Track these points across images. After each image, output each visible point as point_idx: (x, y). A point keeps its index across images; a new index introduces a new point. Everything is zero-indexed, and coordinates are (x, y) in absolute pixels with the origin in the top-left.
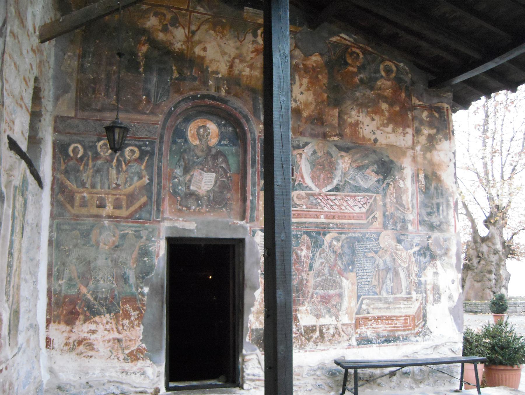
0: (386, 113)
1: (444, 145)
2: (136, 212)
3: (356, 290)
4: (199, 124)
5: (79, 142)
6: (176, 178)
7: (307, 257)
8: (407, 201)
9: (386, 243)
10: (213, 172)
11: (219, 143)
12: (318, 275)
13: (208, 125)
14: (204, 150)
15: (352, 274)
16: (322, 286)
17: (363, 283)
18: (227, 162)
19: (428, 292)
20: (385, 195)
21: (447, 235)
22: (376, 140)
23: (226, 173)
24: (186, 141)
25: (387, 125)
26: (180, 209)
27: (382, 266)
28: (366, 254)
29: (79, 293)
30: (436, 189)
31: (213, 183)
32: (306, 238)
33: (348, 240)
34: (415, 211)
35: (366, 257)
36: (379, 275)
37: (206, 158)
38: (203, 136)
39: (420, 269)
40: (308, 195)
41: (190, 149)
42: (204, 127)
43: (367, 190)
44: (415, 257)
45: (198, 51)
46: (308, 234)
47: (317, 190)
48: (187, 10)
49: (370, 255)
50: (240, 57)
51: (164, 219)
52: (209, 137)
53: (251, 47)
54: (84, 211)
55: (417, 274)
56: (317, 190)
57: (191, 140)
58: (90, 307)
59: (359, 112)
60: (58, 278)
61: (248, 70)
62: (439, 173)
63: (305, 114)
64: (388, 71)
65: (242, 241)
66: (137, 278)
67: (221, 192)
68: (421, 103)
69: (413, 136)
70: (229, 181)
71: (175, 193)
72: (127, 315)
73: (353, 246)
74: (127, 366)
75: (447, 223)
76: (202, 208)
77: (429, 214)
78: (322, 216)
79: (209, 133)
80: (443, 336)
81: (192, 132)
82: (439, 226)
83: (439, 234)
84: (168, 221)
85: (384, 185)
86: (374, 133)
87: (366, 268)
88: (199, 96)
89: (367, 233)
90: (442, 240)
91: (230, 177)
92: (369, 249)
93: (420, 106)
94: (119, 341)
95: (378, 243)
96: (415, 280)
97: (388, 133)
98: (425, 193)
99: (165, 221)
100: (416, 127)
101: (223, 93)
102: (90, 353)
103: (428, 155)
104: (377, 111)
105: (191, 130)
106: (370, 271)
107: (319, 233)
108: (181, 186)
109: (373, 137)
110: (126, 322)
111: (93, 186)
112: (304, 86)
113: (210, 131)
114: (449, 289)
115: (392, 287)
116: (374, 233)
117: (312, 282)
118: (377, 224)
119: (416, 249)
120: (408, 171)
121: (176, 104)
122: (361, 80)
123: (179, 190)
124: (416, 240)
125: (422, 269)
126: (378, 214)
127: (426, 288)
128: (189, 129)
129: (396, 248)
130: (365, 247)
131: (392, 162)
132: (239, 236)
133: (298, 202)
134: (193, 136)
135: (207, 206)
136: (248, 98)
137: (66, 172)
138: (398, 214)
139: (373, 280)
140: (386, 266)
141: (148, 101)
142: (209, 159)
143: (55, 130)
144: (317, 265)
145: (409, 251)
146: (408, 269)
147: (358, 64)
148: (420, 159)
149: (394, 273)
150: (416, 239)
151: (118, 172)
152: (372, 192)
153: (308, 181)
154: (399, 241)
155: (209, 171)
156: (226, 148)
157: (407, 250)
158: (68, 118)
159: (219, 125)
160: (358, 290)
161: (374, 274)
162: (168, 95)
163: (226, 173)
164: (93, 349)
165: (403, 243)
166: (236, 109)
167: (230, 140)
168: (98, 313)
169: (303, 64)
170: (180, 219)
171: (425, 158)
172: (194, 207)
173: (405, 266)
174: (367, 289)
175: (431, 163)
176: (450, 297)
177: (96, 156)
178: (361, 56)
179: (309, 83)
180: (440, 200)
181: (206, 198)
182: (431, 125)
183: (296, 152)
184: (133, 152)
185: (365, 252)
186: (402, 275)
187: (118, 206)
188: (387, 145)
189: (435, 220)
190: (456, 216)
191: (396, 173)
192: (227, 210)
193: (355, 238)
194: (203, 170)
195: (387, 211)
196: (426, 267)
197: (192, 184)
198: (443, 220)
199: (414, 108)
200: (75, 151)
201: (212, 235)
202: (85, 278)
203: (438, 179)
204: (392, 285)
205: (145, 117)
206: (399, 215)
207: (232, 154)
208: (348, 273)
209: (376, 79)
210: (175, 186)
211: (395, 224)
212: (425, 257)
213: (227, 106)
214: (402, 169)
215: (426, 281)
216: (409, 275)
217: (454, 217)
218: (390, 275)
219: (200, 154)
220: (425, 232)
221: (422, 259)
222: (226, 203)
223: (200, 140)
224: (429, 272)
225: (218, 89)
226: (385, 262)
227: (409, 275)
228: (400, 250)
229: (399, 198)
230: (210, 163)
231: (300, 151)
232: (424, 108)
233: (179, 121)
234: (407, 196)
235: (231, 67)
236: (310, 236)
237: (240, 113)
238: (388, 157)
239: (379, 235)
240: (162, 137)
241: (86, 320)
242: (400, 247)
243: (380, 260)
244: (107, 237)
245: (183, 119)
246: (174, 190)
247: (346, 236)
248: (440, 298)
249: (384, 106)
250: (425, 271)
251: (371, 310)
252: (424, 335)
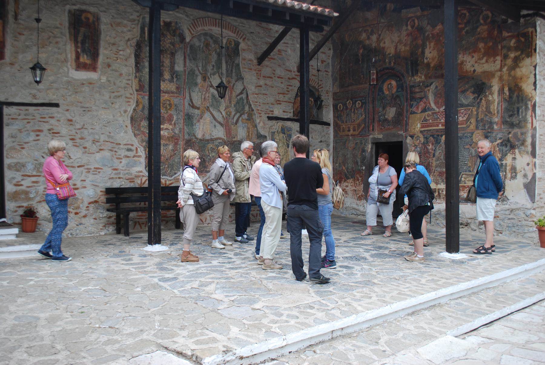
0: (482, 50)
1: (528, 61)
2: (360, 132)
5: (341, 103)
7: (432, 149)
8: (494, 109)
11: (397, 91)
12: (438, 159)
16: (440, 166)
18: (400, 100)
19: (508, 171)
20: (478, 108)
21: (524, 130)
22: (474, 71)
23: (400, 106)
24: (383, 93)
25: (482, 58)
27: (474, 154)
29: (342, 169)
30: (518, 97)
32: (431, 138)
34: (500, 115)
40: (433, 113)
43: (468, 105)
45: (382, 45)
46: (433, 136)
47: (437, 110)
48: (377, 23)
49: (467, 147)
50: (400, 41)
51: (371, 134)
53: (405, 33)
54: (343, 134)
56: (437, 110)
58: (346, 175)
59: (464, 55)
60: (336, 163)
61: (403, 47)
62: (520, 85)
63: (432, 65)
64: (486, 18)
65: (402, 142)
66: (361, 162)
68: (510, 34)
69: (501, 61)
71: (379, 121)
72: (358, 180)
74: (358, 202)
75: (525, 121)
77: (511, 116)
78: (440, 125)
80: (518, 203)
82: (518, 124)
83: (518, 130)
85: (478, 100)
86: (473, 66)
90: (519, 134)
93: (508, 37)
94: (355, 191)
95: (472, 139)
97: (483, 64)
98: (508, 102)
100: (504, 54)
101: (392, 64)
102: (347, 195)
103: (513, 73)
104: (476, 50)
107: (438, 135)
109: (472, 69)
110: (358, 182)
111: (346, 122)
112: (432, 48)
114: (524, 169)
117: (434, 164)
118: (472, 127)
119: (499, 141)
120: (496, 88)
122: (467, 32)
124: (499, 136)
125: (504, 156)
126: (473, 121)
127: (506, 169)
131: (484, 84)
132: (400, 140)
133: (428, 119)
137: (338, 117)
138: (487, 119)
141: (364, 77)
143: (333, 99)
144: (437, 154)
147: (465, 21)
148: (505, 77)
151: (354, 114)
152: (470, 106)
153: (433, 105)
155: (393, 107)
158: (338, 93)
159: (396, 81)
163: (400, 106)
164: (347, 194)
168: (348, 178)
169: (432, 34)
171: (510, 75)
175: (515, 78)
176: (525, 176)
177: (347, 109)
178: (467, 14)
179: (434, 44)
180: (521, 104)
182: (516, 49)
183: (426, 90)
184: (359, 103)
187: (354, 130)
188: (482, 72)
189: (515, 120)
190: (533, 115)
191: (487, 90)
195: (478, 117)
196: (507, 154)
198: (522, 120)
199: (504, 39)
200: (340, 108)
201: (389, 141)
202: (344, 162)
203: (520, 89)
205: (362, 86)
206: (487, 119)
209: (477, 27)
211: (484, 125)
212: (506, 147)
214: (491, 87)
217: (532, 116)
219: (389, 98)
221: (504, 148)
224: (509, 157)
225: (390, 63)
229: (488, 108)
231: (429, 88)
232: (512, 37)
234: (494, 106)
235: (396, 49)
236: (434, 138)
238: (481, 80)
239: (472, 134)
240: (369, 94)
241: (345, 181)
244: (351, 145)
248: (516, 176)
249: (481, 45)
251: (466, 181)
252: (503, 201)
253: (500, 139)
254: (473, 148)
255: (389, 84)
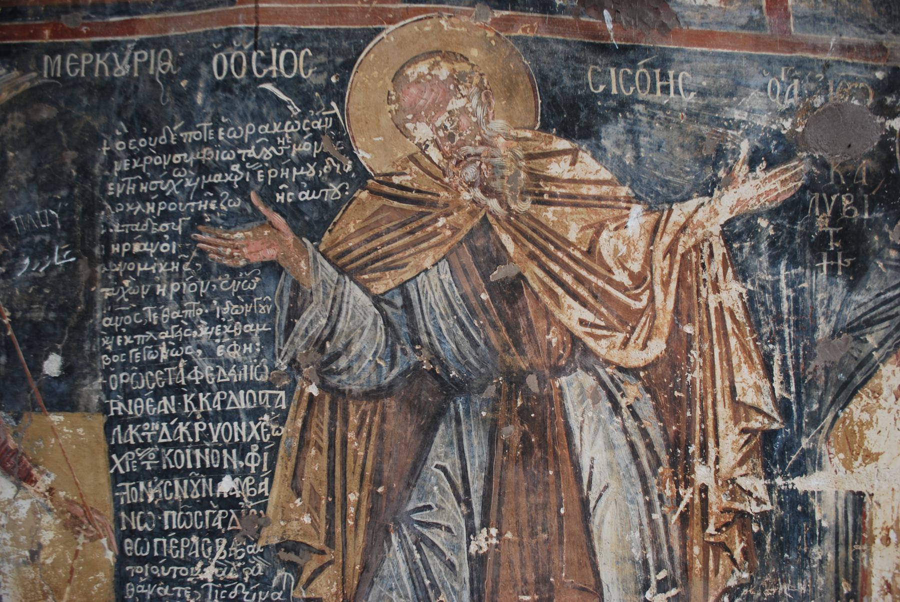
3: (104, 578)
9: (423, 132)
15: (69, 434)
17: (172, 518)
28: (204, 237)
33: (46, 113)
35: (206, 273)
36: (336, 449)
39: (804, 386)
44: (742, 274)
49: (248, 245)
55: (769, 436)
73: (84, 170)
87: (205, 371)
89: (228, 38)
92: (243, 190)
95: (339, 133)
96: (737, 492)
106: (241, 401)
115: (478, 562)
116: (295, 40)
119: (753, 190)
124: (760, 109)
129: (535, 177)
130: (202, 168)
139: (277, 493)
140: (407, 358)
145: (679, 213)
146: (667, 385)
149: (511, 432)
150: (755, 99)
154: (571, 115)
157: (659, 197)
160: (121, 579)
161: (289, 432)
165: (612, 134)
173: (636, 357)
174: (210, 573)
185: (198, 218)
186: (599, 445)
193: (105, 88)
196: (867, 368)
204: (482, 542)
208: (34, 422)
212: (856, 275)
215: (858, 501)
216: (677, 445)
218: (460, 451)
220: (851, 35)
221: (825, 291)
226: (400, 314)
227: (677, 445)
228: (574, 201)
242: (578, 167)
243: (354, 294)
247: (26, 82)
250: (856, 409)
253: (771, 154)
254: (345, 268)
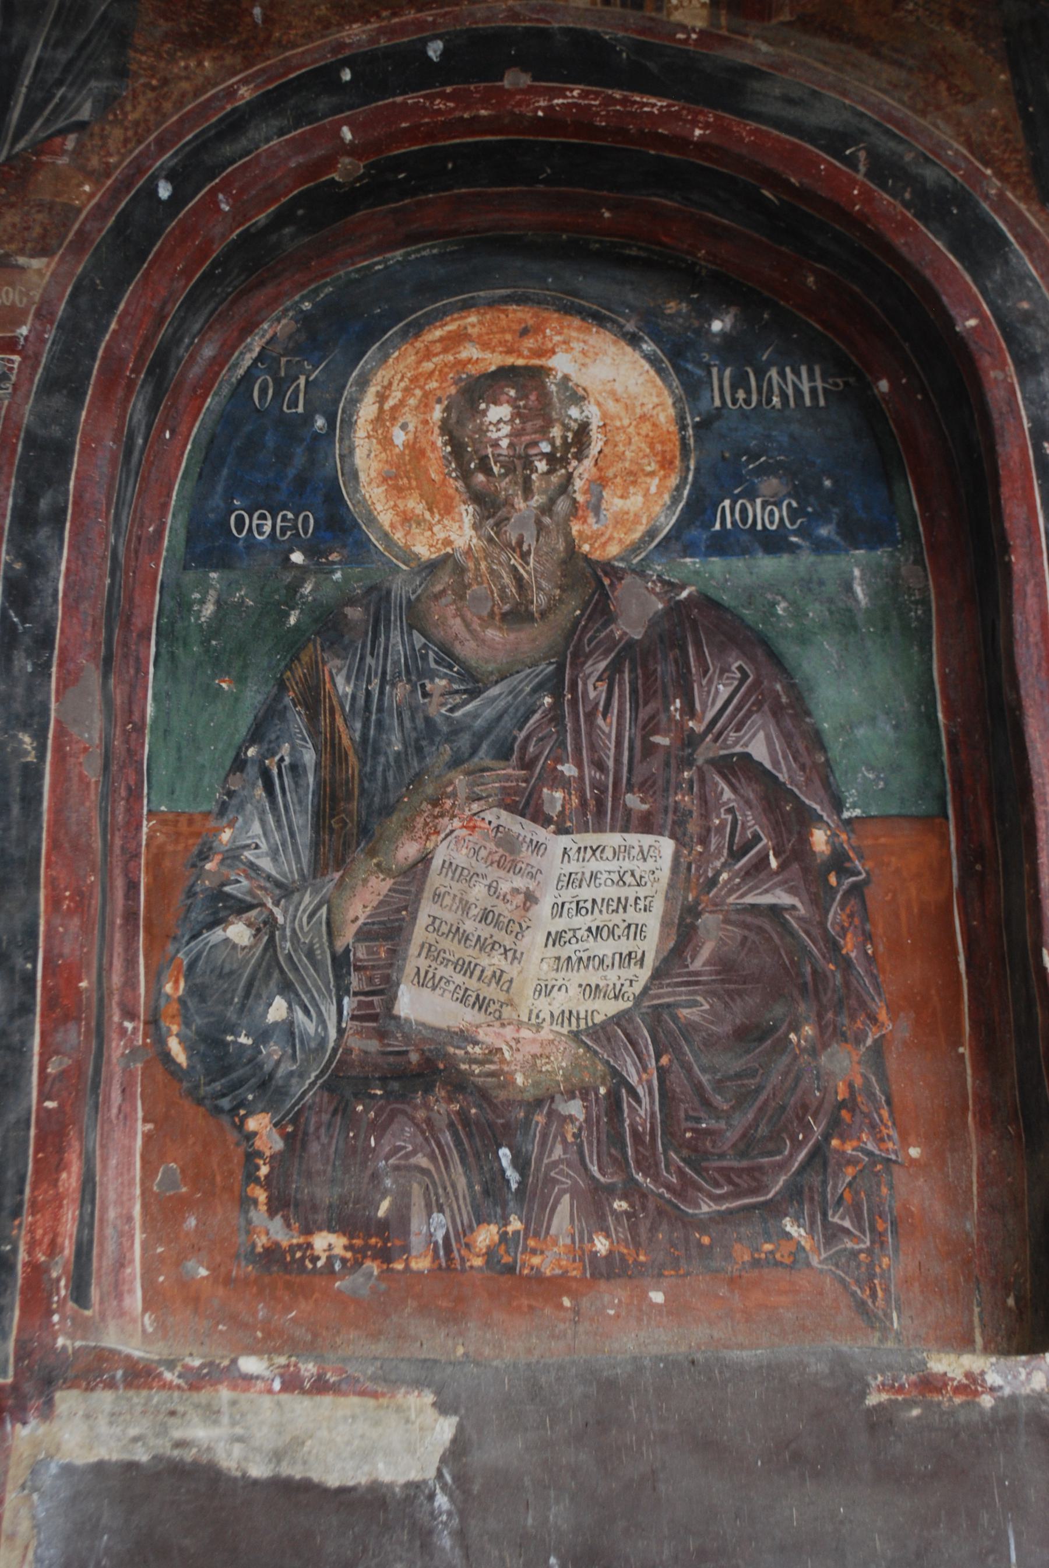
4: (470, 351)
6: (241, 908)
10: (647, 825)
13: (561, 363)
14: (539, 600)
18: (792, 710)
23: (790, 821)
24: (338, 524)
26: (272, 1254)
31: (650, 945)
37: (554, 684)
38: (520, 464)
41: (377, 610)
42: (526, 379)
52: (583, 471)
57: (385, 518)
67: (749, 1035)
70: (835, 914)
71: (223, 1078)
76: (537, 1227)
79: (583, 429)
81: (399, 437)
84: (105, 1398)
88: (435, 50)
91: (839, 862)
99: (67, 1400)
105: (387, 423)
108: (286, 988)
113: (593, 413)
121: (203, 145)
123: (263, 1035)
128: (367, 410)
134: (404, 472)
135: (594, 1203)
136: (960, 42)
142: (596, 692)
155: (597, 812)
156: (768, 565)
159: (678, 356)
162: (121, 73)
163: (790, 821)
166: (837, 141)
167: (803, 489)
170: (250, 1364)
172: (440, 1224)
181: (575, 1108)
192: (832, 1234)
194: (531, 809)
197: (415, 961)
207: (846, 622)
210: (218, 998)
213: (745, 129)
219: (488, 643)
222: (819, 1155)
223: (489, 506)
230: (607, 726)
233: (256, 344)
237: (883, 170)
245: (306, 320)
246: (211, 1044)
255: (478, 390)
